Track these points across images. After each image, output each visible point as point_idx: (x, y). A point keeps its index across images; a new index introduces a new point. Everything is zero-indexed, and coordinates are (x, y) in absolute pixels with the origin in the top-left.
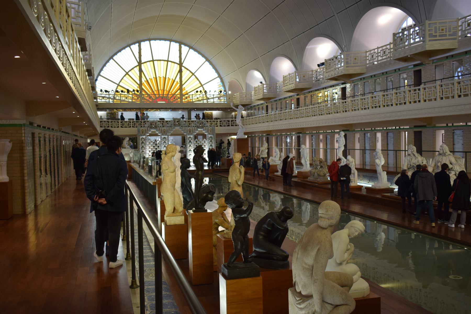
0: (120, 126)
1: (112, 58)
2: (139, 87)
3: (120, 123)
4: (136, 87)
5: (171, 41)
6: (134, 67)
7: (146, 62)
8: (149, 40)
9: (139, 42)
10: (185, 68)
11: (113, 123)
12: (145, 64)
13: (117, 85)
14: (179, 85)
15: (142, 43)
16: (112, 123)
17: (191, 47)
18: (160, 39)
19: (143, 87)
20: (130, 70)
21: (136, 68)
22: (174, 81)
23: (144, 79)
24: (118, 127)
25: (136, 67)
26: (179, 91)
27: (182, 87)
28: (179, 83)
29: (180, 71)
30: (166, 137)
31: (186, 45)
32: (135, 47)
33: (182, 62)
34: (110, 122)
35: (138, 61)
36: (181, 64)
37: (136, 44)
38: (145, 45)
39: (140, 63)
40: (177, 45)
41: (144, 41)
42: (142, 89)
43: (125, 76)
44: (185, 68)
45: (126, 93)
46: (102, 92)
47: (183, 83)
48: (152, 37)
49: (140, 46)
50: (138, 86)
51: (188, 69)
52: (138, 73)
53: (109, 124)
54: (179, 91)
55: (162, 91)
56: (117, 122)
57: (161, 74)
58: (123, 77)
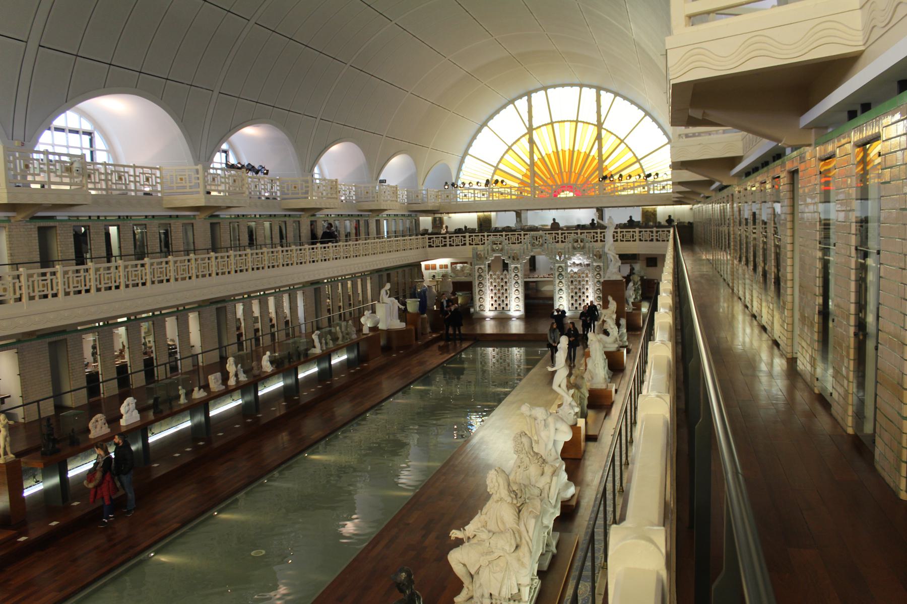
0: (467, 242)
1: (485, 124)
2: (530, 168)
3: (467, 239)
4: (524, 169)
5: (581, 86)
6: (521, 137)
7: (540, 127)
8: (545, 88)
9: (529, 94)
10: (607, 131)
11: (454, 238)
12: (538, 130)
13: (494, 169)
14: (596, 161)
15: (533, 95)
16: (452, 240)
17: (616, 94)
18: (563, 85)
19: (536, 169)
20: (515, 143)
21: (524, 138)
22: (589, 155)
23: (536, 156)
24: (465, 244)
25: (524, 136)
26: (597, 172)
27: (602, 165)
28: (597, 158)
29: (599, 138)
30: (519, 266)
31: (607, 90)
32: (522, 103)
33: (602, 121)
34: (448, 238)
35: (528, 126)
36: (599, 125)
37: (523, 98)
38: (538, 98)
39: (530, 129)
40: (594, 91)
41: (536, 91)
42: (534, 174)
43: (506, 152)
44: (607, 131)
45: (483, 187)
46: (446, 187)
47: (604, 158)
48: (549, 83)
49: (529, 101)
50: (528, 167)
51: (612, 133)
52: (527, 146)
53: (445, 242)
54: (597, 172)
55: (568, 173)
56: (462, 236)
57: (565, 145)
58: (504, 155)
